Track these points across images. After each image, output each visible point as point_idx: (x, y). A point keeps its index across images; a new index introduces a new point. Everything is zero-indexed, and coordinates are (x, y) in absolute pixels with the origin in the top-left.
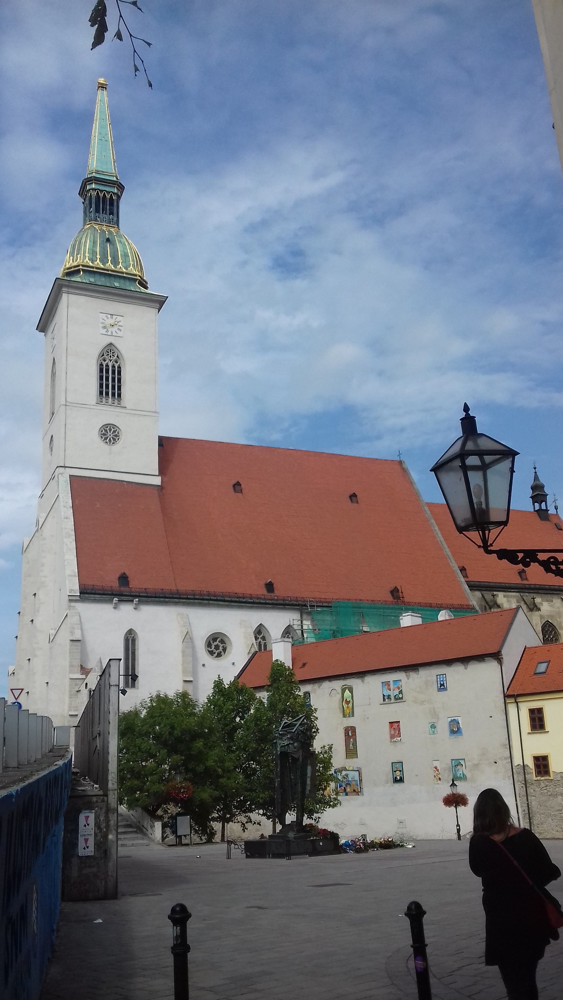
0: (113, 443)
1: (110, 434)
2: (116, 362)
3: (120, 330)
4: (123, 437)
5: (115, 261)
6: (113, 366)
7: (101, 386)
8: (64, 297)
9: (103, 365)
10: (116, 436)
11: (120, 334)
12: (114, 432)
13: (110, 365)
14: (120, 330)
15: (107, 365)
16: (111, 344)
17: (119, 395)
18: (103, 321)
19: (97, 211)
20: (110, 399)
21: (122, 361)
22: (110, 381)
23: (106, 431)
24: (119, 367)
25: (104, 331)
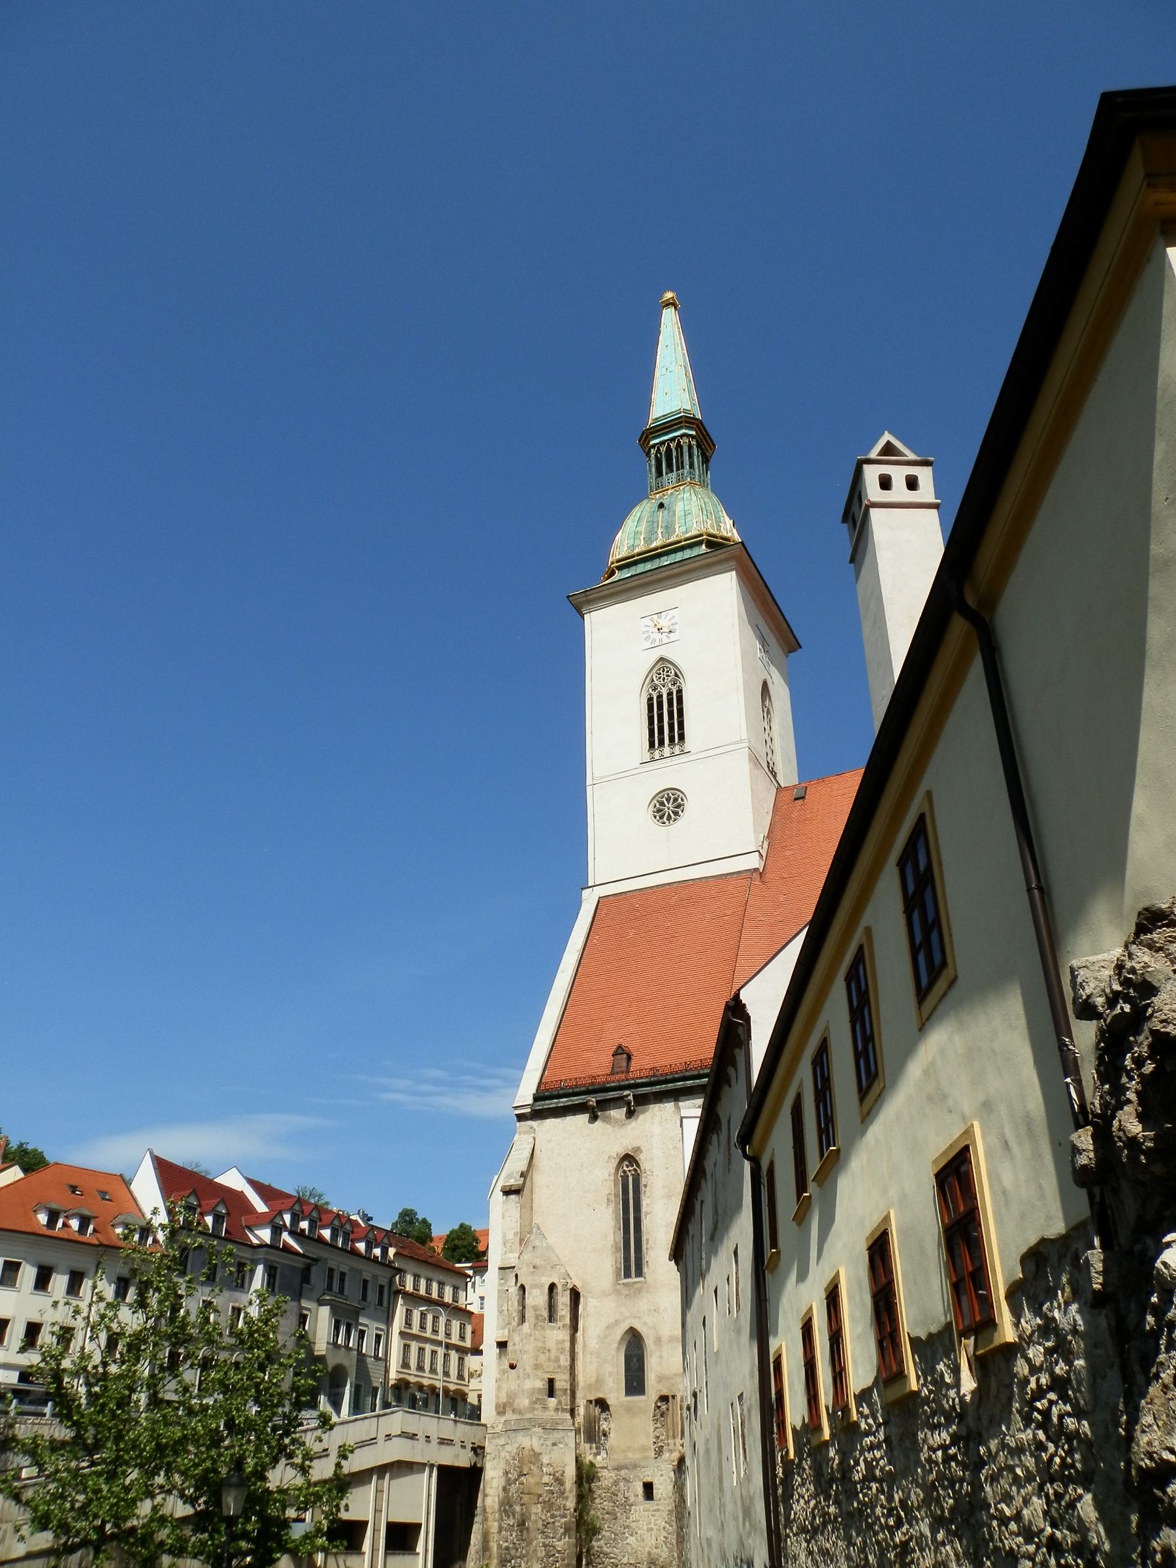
1: (668, 806)
4: (688, 805)
5: (669, 529)
6: (670, 694)
12: (676, 800)
15: (660, 697)
16: (662, 659)
17: (682, 737)
20: (667, 750)
22: (666, 721)
23: (662, 804)
24: (680, 691)
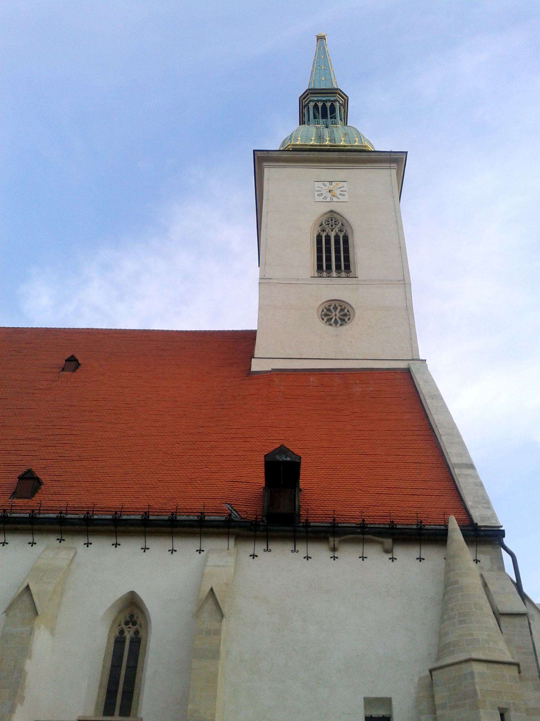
0: (341, 325)
1: (337, 314)
2: (341, 231)
3: (344, 195)
7: (319, 259)
8: (266, 170)
9: (321, 236)
10: (345, 315)
11: (342, 199)
12: (342, 310)
13: (332, 235)
14: (344, 195)
17: (347, 267)
18: (320, 189)
19: (315, 117)
20: (334, 274)
21: (349, 231)
23: (328, 310)
25: (321, 199)
